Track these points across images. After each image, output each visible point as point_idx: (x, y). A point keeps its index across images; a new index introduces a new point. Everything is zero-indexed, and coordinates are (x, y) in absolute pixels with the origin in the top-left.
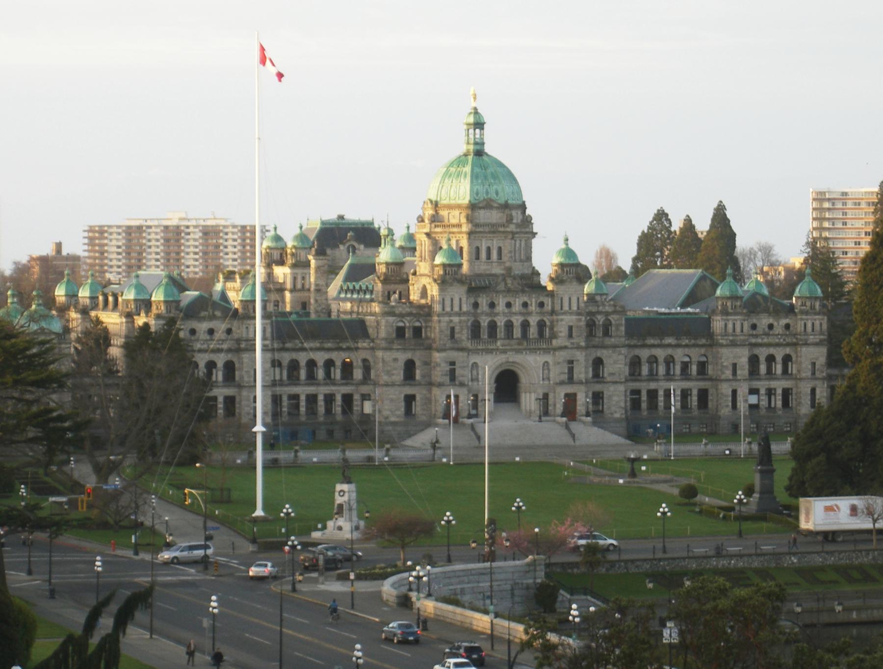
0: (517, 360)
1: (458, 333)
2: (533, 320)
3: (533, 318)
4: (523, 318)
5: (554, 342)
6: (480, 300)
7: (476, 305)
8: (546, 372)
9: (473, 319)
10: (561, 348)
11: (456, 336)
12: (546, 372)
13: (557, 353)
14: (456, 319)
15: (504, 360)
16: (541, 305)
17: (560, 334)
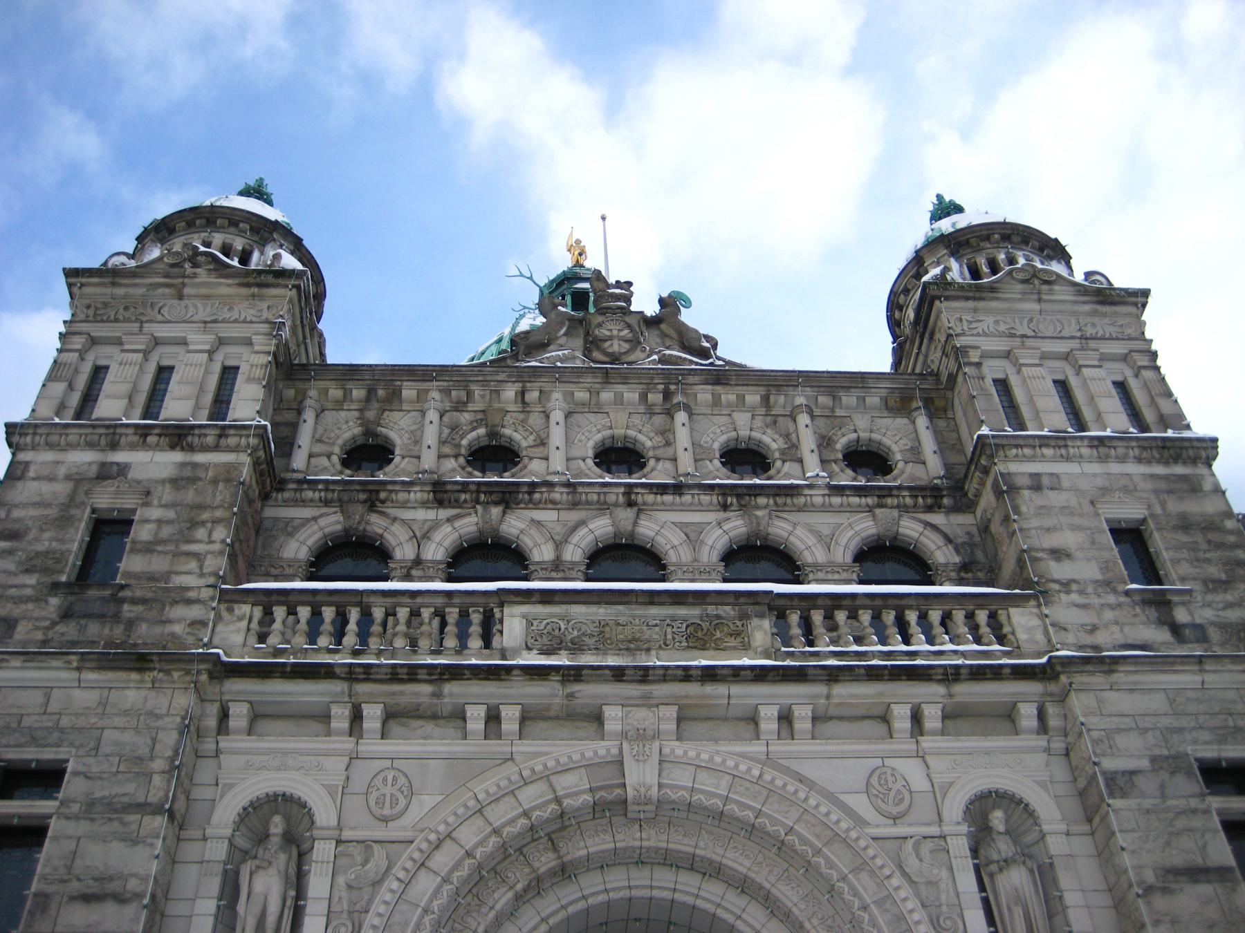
0: (712, 788)
1: (148, 549)
2: (822, 537)
3: (823, 522)
4: (736, 527)
5: (1022, 620)
6: (397, 428)
7: (370, 452)
8: (1015, 880)
9: (332, 522)
10: (1097, 662)
11: (132, 563)
12: (1015, 880)
13: (1078, 702)
14: (155, 463)
15: (575, 788)
16: (866, 459)
17: (1059, 570)
